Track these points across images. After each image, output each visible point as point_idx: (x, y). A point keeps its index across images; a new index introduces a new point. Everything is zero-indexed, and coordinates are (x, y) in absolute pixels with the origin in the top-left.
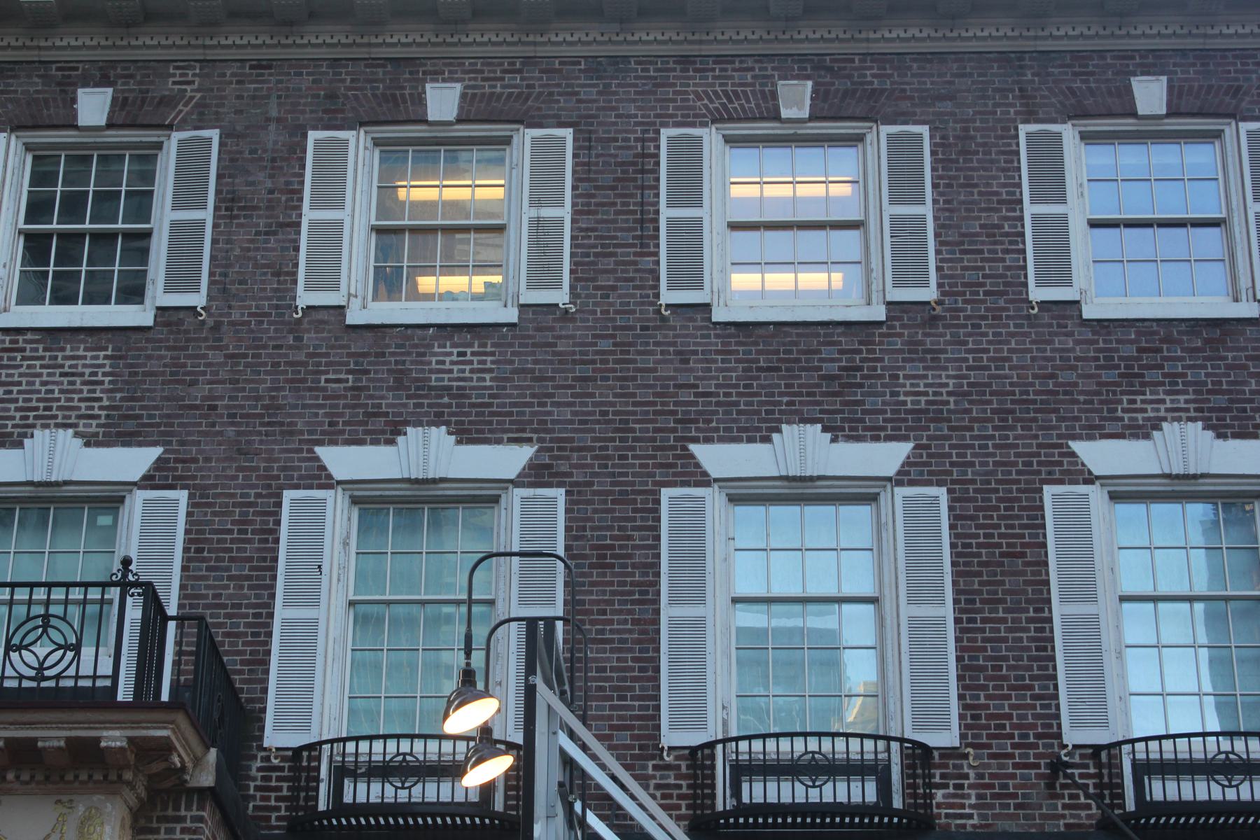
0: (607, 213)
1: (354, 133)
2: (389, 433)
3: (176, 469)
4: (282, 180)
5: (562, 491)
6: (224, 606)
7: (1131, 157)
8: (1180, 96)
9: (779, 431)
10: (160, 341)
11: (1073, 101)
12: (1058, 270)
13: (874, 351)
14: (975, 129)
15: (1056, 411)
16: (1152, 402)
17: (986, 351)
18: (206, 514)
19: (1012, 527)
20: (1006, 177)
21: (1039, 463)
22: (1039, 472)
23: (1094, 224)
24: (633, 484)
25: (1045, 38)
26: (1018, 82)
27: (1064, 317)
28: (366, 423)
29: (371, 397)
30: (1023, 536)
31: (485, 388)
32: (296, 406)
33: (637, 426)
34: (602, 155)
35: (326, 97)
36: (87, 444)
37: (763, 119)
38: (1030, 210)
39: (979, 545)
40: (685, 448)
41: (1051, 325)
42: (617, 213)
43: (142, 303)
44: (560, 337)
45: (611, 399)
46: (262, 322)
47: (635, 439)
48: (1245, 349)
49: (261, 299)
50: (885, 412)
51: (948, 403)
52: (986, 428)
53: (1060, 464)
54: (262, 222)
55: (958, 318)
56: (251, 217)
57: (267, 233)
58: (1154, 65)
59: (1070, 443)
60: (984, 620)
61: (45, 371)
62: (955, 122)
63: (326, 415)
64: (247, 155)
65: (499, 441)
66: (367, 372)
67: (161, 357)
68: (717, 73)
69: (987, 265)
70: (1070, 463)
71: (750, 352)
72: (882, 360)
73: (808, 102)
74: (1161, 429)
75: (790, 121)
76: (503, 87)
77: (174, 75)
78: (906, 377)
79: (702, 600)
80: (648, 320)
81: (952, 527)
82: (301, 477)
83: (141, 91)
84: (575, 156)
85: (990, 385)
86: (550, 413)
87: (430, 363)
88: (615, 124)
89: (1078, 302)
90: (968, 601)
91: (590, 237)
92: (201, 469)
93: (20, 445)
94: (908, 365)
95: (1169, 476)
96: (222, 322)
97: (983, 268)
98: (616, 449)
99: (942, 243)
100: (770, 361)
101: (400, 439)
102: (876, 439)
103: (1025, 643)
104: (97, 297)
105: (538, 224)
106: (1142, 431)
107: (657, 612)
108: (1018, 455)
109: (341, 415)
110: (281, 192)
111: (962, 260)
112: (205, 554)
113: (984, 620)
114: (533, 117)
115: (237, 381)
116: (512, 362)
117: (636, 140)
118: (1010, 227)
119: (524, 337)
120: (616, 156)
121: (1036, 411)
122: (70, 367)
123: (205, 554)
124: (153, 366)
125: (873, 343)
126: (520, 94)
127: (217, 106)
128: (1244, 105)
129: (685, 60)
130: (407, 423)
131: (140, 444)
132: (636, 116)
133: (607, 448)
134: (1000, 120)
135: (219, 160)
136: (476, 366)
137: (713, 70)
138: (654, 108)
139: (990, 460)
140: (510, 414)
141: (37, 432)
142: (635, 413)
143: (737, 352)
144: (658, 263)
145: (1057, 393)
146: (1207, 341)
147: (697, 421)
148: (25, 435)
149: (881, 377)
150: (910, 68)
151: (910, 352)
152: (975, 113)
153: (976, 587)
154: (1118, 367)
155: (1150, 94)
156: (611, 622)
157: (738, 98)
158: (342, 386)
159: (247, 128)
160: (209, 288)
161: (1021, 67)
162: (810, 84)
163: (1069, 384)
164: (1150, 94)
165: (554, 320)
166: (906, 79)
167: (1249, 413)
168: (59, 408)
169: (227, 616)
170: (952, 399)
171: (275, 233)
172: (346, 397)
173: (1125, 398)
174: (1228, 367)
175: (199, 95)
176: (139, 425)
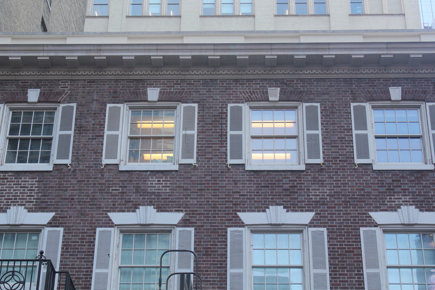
0: (209, 132)
1: (123, 105)
2: (134, 208)
3: (59, 220)
4: (98, 121)
5: (193, 228)
6: (75, 268)
7: (389, 114)
8: (406, 94)
9: (268, 208)
10: (55, 176)
11: (369, 95)
12: (365, 153)
13: (301, 181)
14: (336, 105)
15: (364, 202)
16: (397, 199)
17: (340, 181)
19: (349, 242)
20: (346, 121)
21: (359, 220)
22: (358, 223)
23: (377, 137)
24: (218, 226)
25: (360, 74)
26: (351, 89)
27: (367, 169)
28: (126, 205)
29: (127, 195)
30: (353, 245)
31: (167, 193)
32: (101, 199)
33: (219, 206)
34: (208, 113)
35: (113, 92)
36: (29, 211)
37: (263, 101)
38: (355, 132)
39: (338, 248)
40: (236, 214)
41: (362, 172)
42: (213, 133)
43: (49, 162)
44: (193, 175)
45: (210, 197)
46: (90, 169)
47: (219, 211)
48: (429, 180)
49: (90, 161)
50: (305, 202)
51: (327, 199)
52: (340, 207)
53: (366, 220)
54: (90, 135)
55: (330, 169)
56: (87, 133)
57: (92, 139)
58: (397, 83)
59: (369, 213)
60: (340, 275)
61: (15, 186)
62: (329, 102)
64: (86, 112)
65: (171, 211)
66: (126, 187)
67: (55, 181)
68: (247, 85)
69: (340, 151)
70: (369, 220)
71: (258, 181)
72: (304, 184)
73: (278, 95)
74: (401, 208)
75: (272, 101)
76: (174, 89)
77: (61, 85)
78: (312, 189)
79: (241, 267)
80: (223, 169)
81: (328, 242)
82: (103, 223)
83: (50, 90)
84: (198, 113)
85: (341, 192)
86: (189, 201)
87: (148, 184)
88: (212, 102)
89: (371, 164)
90: (334, 268)
91: (203, 141)
92: (68, 220)
93: (5, 211)
94: (313, 185)
95: (403, 224)
96: (76, 170)
97: (339, 152)
98: (212, 214)
99: (324, 144)
100: (265, 184)
101: (137, 210)
102: (302, 211)
103: (354, 283)
104: (33, 160)
105: (185, 136)
106: (394, 209)
107: (226, 271)
108: (351, 217)
109: (117, 202)
110: (97, 125)
111: (331, 149)
113: (340, 275)
114: (184, 99)
115: (81, 190)
116: (176, 184)
117: (219, 108)
118: (348, 138)
119: (181, 175)
120: (212, 113)
121: (357, 202)
122: (24, 185)
123: (69, 250)
124: (52, 184)
125: (301, 178)
126: (180, 92)
127: (76, 95)
128: (428, 97)
129: (236, 81)
130: (140, 205)
131: (47, 212)
132: (219, 99)
133: (209, 214)
134: (344, 102)
135: (76, 114)
136: (164, 185)
137: (246, 84)
138: (226, 97)
139: (342, 218)
140: (175, 202)
141: (12, 207)
142: (218, 202)
143: (254, 181)
144: (227, 150)
145: (365, 195)
146: (416, 178)
147: (240, 204)
148: (7, 208)
149: (303, 189)
150: (313, 84)
151: (314, 181)
152: (336, 99)
153: (337, 263)
154: (385, 186)
155: (396, 93)
156: (210, 274)
157: (254, 94)
158: (117, 191)
159: (86, 103)
160: (72, 158)
161: (351, 83)
162: (279, 89)
163: (369, 192)
164: (396, 93)
165: (191, 169)
166: (313, 87)
167: (431, 203)
168: (19, 199)
169: (76, 272)
170: (328, 197)
171: (95, 139)
172: (118, 195)
173: (388, 197)
174: (423, 187)
175: (69, 92)
176: (47, 205)
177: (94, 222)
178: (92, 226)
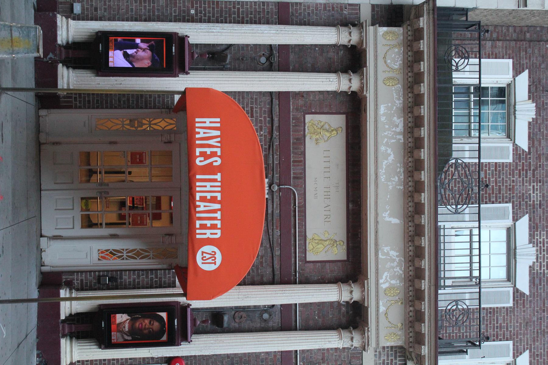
18: (504, 313)
32: (544, 341)
36: (530, 267)
63: (541, 353)
82: (517, 346)
92: (521, 309)
93: (530, 242)
109: (541, 358)
131: (530, 286)
141: (535, 249)
148: (534, 244)
176: (537, 284)
178: (514, 335)
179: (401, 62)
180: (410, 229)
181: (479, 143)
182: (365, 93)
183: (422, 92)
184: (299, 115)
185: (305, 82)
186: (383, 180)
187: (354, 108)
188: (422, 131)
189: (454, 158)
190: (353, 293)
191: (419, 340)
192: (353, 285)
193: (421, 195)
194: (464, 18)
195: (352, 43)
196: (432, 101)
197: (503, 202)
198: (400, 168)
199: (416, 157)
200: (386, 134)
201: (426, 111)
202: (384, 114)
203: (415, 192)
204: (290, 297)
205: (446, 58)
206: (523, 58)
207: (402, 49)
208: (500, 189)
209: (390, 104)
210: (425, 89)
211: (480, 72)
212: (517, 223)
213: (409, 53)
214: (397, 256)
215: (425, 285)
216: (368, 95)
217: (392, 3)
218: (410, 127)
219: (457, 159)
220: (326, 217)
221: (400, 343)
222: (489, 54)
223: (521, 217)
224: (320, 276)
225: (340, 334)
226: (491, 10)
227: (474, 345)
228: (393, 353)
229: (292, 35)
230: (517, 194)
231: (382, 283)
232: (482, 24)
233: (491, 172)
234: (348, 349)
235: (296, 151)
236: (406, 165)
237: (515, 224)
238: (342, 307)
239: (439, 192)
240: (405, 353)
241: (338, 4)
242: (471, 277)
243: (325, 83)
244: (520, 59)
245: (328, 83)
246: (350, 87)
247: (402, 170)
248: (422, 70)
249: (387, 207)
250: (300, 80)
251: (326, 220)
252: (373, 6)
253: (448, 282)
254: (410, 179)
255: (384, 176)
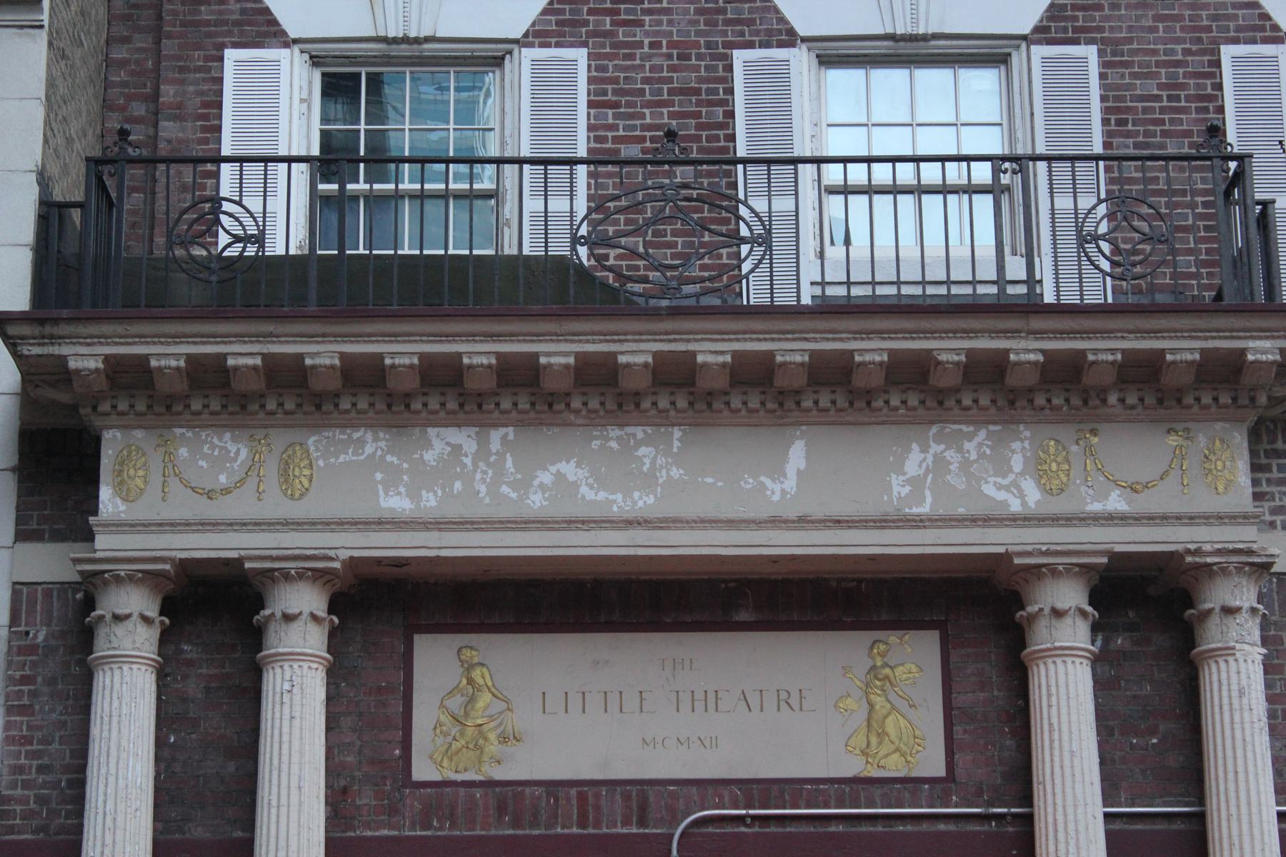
3: (1075, 18)
18: (1123, 76)
82: (1239, 29)
112: (1130, 127)
123: (1130, 127)
177: (1205, 23)
178: (1199, 40)
179: (228, 436)
180: (824, 401)
181: (520, 161)
182: (337, 565)
183: (337, 362)
184: (413, 804)
185: (294, 783)
186: (651, 500)
187: (388, 606)
188: (477, 360)
189: (574, 249)
190: (1060, 605)
191: (1224, 373)
192: (1032, 609)
193: (705, 365)
194: (76, 214)
195: (153, 612)
196: (369, 328)
197: (727, 81)
198: (608, 439)
199: (565, 384)
200: (483, 489)
201: (402, 349)
202: (414, 495)
203: (693, 385)
204: (1082, 837)
205: (214, 278)
206: (221, 13)
207: (178, 431)
208: (682, 91)
209: (379, 476)
210: (323, 353)
211: (266, 160)
212: (802, 30)
213: (196, 405)
214: (924, 450)
215: (1028, 351)
216: (344, 554)
217: (13, 470)
218: (461, 405)
219: (575, 240)
220: (783, 705)
221: (1240, 439)
222: (205, 129)
223: (782, 20)
224: (998, 726)
225: (1213, 654)
226: (47, 122)
227: (1239, 178)
228: (1274, 463)
229: (119, 833)
230: (698, 33)
231: (1024, 504)
232: (97, 153)
233: (621, 123)
234: (1264, 627)
235: (543, 817)
236: (596, 419)
237: (804, 40)
238: (1112, 646)
239: (692, 302)
240: (1274, 421)
241: (9, 664)
242: (994, 189)
243: (297, 708)
244: (225, 23)
245: (297, 698)
246: (314, 617)
247: (615, 432)
248: (258, 361)
249: (749, 483)
250: (284, 800)
251: (797, 707)
252: (23, 535)
253: (1016, 268)
254: (646, 404)
255: (636, 495)
